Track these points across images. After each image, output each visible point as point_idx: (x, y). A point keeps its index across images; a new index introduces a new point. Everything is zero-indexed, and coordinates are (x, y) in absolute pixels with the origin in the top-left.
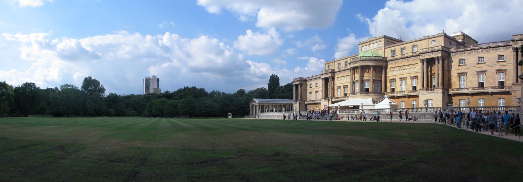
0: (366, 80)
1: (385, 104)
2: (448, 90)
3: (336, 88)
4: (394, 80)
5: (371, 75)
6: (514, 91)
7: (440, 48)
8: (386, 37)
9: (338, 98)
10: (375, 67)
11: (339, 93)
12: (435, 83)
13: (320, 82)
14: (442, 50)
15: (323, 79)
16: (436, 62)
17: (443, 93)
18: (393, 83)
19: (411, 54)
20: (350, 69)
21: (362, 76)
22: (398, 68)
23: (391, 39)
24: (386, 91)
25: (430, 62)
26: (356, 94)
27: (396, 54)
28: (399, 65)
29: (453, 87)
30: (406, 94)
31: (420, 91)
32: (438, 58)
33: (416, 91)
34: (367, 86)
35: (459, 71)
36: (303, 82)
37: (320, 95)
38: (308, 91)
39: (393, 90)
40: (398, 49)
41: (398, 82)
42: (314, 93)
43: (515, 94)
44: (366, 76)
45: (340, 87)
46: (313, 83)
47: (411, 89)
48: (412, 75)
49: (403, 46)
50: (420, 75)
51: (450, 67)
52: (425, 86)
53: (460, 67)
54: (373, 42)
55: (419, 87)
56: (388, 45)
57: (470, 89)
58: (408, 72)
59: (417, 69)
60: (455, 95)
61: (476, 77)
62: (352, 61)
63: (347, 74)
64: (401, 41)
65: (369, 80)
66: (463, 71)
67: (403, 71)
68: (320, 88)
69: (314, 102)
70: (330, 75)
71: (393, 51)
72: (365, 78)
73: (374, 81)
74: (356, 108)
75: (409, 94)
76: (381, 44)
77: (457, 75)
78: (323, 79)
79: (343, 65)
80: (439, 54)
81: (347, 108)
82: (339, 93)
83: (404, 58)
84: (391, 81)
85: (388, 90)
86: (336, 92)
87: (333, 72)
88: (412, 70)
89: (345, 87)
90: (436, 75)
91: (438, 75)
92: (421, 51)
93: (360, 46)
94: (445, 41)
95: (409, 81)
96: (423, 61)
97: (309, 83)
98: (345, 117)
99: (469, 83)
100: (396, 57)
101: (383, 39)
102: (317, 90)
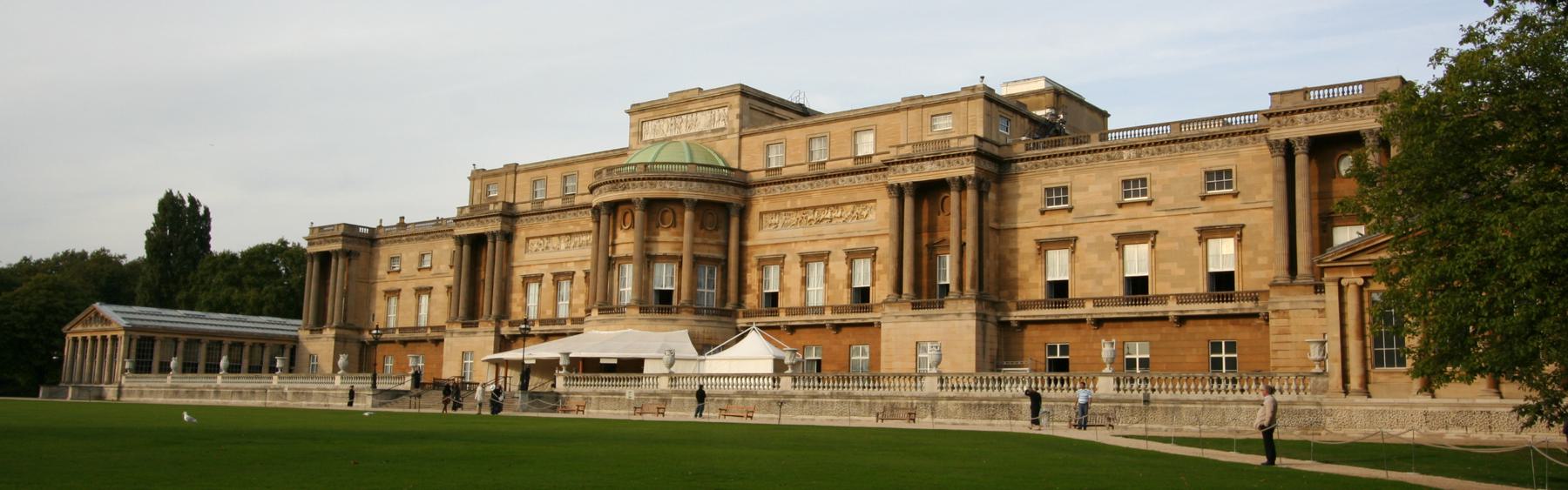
1: (751, 355)
2: (997, 305)
3: (517, 280)
4: (779, 260)
5: (686, 238)
6: (1282, 313)
7: (970, 143)
8: (745, 92)
10: (700, 206)
11: (532, 303)
12: (948, 276)
14: (979, 154)
15: (460, 240)
16: (954, 196)
17: (981, 318)
19: (849, 164)
20: (596, 210)
21: (647, 241)
22: (794, 217)
24: (740, 302)
25: (930, 192)
26: (620, 310)
28: (799, 204)
29: (1022, 296)
30: (828, 316)
31: (887, 309)
32: (962, 183)
33: (869, 309)
34: (664, 277)
35: (1045, 234)
36: (360, 244)
37: (433, 310)
38: (381, 287)
39: (773, 299)
41: (795, 270)
42: (408, 297)
43: (1283, 322)
44: (665, 242)
45: (538, 278)
46: (408, 253)
47: (845, 298)
49: (817, 130)
50: (885, 246)
51: (1004, 211)
53: (1047, 219)
55: (881, 292)
56: (753, 123)
57: (1089, 305)
58: (834, 232)
60: (1023, 324)
61: (1115, 254)
62: (605, 178)
63: (571, 229)
64: (803, 112)
65: (677, 259)
66: (1058, 233)
67: (817, 229)
68: (439, 275)
69: (407, 336)
70: (494, 226)
73: (697, 261)
74: (633, 366)
75: (838, 318)
76: (727, 116)
78: (460, 240)
79: (555, 189)
80: (967, 169)
81: (590, 366)
82: (533, 302)
83: (822, 176)
84: (763, 264)
85: (751, 300)
86: (516, 296)
87: (510, 214)
88: (852, 226)
90: (954, 246)
91: (962, 245)
92: (893, 154)
94: (988, 116)
95: (839, 267)
96: (899, 192)
97: (385, 252)
98: (602, 405)
99: (1083, 278)
101: (736, 99)
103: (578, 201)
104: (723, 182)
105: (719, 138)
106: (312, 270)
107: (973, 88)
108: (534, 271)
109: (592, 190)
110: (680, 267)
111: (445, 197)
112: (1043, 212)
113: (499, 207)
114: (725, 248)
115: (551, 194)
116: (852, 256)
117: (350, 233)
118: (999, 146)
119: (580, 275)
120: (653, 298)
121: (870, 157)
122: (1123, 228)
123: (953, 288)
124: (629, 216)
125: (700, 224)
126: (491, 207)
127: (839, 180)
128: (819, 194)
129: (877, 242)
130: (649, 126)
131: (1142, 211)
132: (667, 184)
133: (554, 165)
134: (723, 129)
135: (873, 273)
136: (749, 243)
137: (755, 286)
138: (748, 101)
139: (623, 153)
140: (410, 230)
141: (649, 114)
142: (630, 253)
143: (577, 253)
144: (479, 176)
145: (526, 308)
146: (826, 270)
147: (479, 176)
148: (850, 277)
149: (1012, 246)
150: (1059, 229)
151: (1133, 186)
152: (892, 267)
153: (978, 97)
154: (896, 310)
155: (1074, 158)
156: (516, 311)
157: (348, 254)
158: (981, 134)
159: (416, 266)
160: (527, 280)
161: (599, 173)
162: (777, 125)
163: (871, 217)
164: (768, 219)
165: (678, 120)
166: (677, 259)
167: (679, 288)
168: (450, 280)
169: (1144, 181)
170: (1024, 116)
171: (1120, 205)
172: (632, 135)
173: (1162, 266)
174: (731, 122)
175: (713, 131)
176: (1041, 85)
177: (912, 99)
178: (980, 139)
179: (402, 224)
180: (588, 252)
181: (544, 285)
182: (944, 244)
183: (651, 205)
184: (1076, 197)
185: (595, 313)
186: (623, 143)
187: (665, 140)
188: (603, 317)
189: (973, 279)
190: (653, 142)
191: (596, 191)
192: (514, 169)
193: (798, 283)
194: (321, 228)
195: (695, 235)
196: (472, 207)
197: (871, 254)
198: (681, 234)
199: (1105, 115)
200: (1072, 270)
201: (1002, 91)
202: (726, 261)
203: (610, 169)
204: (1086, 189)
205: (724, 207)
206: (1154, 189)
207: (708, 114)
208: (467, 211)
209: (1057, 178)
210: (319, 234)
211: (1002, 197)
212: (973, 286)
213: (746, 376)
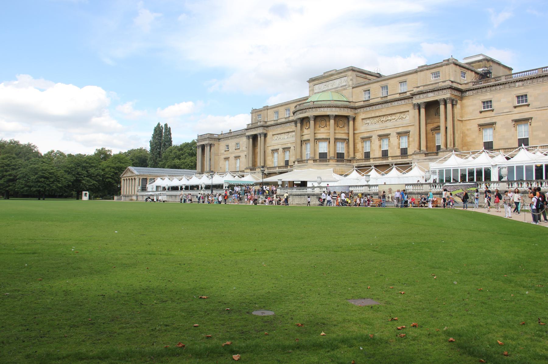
3: (269, 151)
4: (369, 138)
5: (332, 130)
8: (353, 70)
10: (336, 117)
15: (248, 137)
16: (442, 107)
19: (397, 96)
20: (295, 122)
25: (432, 107)
27: (371, 97)
28: (377, 114)
31: (414, 157)
32: (445, 102)
34: (323, 148)
35: (482, 122)
42: (232, 159)
44: (322, 133)
45: (277, 150)
46: (232, 143)
47: (398, 153)
48: (400, 130)
49: (383, 83)
50: (414, 131)
52: (423, 148)
53: (483, 115)
54: (332, 78)
59: (410, 118)
61: (513, 129)
62: (298, 108)
63: (289, 130)
64: (379, 76)
66: (488, 121)
68: (243, 151)
73: (336, 140)
77: (477, 128)
78: (248, 137)
80: (447, 95)
82: (276, 160)
83: (386, 102)
86: (269, 158)
88: (399, 123)
89: (286, 149)
92: (416, 90)
100: (371, 102)
102: (237, 155)
103: (291, 119)
105: (344, 89)
106: (199, 151)
107: (448, 60)
108: (276, 148)
109: (294, 113)
111: (241, 121)
112: (481, 112)
115: (280, 117)
116: (400, 134)
117: (211, 137)
118: (461, 84)
120: (317, 157)
121: (406, 92)
122: (517, 117)
123: (442, 147)
126: (259, 123)
127: (393, 103)
130: (317, 86)
131: (525, 109)
132: (322, 109)
133: (281, 105)
134: (346, 85)
135: (409, 142)
136: (355, 132)
137: (360, 150)
139: (306, 98)
140: (232, 134)
141: (316, 82)
142: (309, 138)
144: (255, 112)
145: (273, 162)
147: (255, 112)
148: (399, 144)
149: (468, 127)
150: (488, 119)
151: (522, 98)
152: (417, 138)
153: (451, 64)
154: (418, 157)
155: (494, 88)
156: (269, 163)
158: (452, 80)
159: (234, 148)
160: (275, 151)
161: (296, 107)
163: (407, 118)
165: (327, 83)
166: (327, 140)
167: (329, 152)
169: (526, 96)
170: (472, 71)
171: (515, 107)
172: (310, 91)
173: (535, 133)
175: (342, 87)
176: (481, 58)
177: (422, 66)
178: (452, 82)
179: (230, 133)
180: (294, 139)
181: (279, 153)
182: (437, 129)
183: (316, 118)
184: (494, 104)
185: (296, 163)
186: (307, 95)
188: (299, 164)
189: (451, 142)
190: (318, 93)
191: (295, 114)
192: (267, 108)
193: (378, 147)
194: (201, 136)
195: (335, 130)
196: (252, 124)
197: (407, 133)
199: (511, 69)
200: (494, 137)
201: (462, 62)
202: (348, 139)
203: (299, 105)
204: (499, 101)
205: (347, 117)
206: (529, 98)
208: (250, 126)
209: (487, 96)
210: (201, 138)
211: (462, 107)
212: (450, 145)
213: (356, 186)
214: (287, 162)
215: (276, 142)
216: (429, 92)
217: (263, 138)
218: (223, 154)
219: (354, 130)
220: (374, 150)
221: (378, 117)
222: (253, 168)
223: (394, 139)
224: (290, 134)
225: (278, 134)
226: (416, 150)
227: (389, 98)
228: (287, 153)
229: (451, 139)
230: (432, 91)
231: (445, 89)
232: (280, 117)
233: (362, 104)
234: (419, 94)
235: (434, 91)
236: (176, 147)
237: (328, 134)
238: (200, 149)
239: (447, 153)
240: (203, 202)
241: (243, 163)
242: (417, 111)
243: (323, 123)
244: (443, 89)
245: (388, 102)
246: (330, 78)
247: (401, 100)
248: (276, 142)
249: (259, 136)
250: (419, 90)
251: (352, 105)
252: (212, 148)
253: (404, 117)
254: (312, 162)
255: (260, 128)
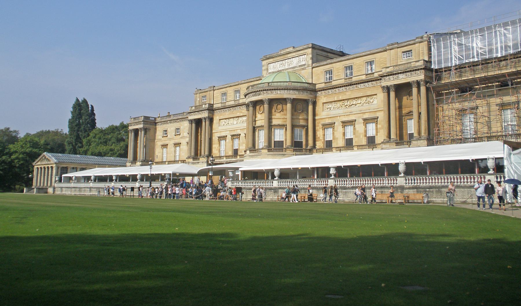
0: (279, 125)
3: (215, 138)
4: (331, 125)
5: (289, 116)
8: (314, 47)
9: (220, 157)
10: (294, 101)
11: (222, 149)
13: (185, 126)
15: (191, 121)
16: (415, 90)
18: (329, 131)
19: (364, 77)
20: (247, 105)
22: (339, 104)
23: (323, 49)
25: (402, 90)
27: (334, 78)
28: (341, 98)
32: (418, 83)
34: (279, 135)
40: (338, 67)
41: (339, 128)
42: (171, 147)
45: (224, 138)
46: (171, 128)
48: (366, 116)
50: (382, 116)
56: (317, 61)
58: (358, 110)
62: (251, 90)
70: (205, 114)
71: (330, 72)
72: (275, 122)
76: (306, 58)
78: (191, 121)
80: (420, 76)
82: (223, 148)
83: (351, 85)
84: (326, 126)
85: (320, 144)
86: (215, 146)
87: (211, 109)
89: (235, 137)
92: (384, 71)
93: (264, 63)
96: (388, 89)
97: (160, 129)
100: (334, 83)
101: (310, 50)
102: (177, 141)
103: (241, 101)
104: (304, 90)
105: (303, 69)
106: (131, 136)
108: (223, 134)
110: (286, 130)
113: (207, 106)
114: (307, 120)
116: (366, 121)
119: (243, 135)
123: (416, 135)
124: (262, 107)
125: (294, 109)
126: (204, 106)
127: (359, 86)
128: (350, 92)
129: (378, 114)
132: (279, 92)
134: (304, 65)
135: (377, 129)
136: (316, 118)
138: (315, 51)
140: (172, 118)
142: (263, 124)
143: (240, 125)
145: (220, 151)
146: (354, 129)
148: (366, 131)
152: (386, 126)
156: (215, 152)
157: (146, 130)
159: (174, 134)
161: (248, 88)
162: (329, 61)
163: (375, 102)
164: (326, 106)
167: (286, 140)
168: (187, 140)
174: (308, 62)
175: (300, 66)
179: (169, 116)
180: (245, 125)
183: (271, 102)
185: (248, 152)
187: (278, 71)
190: (273, 72)
191: (247, 97)
193: (342, 135)
195: (292, 115)
197: (375, 120)
198: (286, 115)
202: (307, 126)
205: (306, 102)
207: (297, 58)
212: (425, 133)
214: (236, 152)
215: (224, 127)
216: (401, 73)
217: (207, 123)
218: (160, 140)
219: (314, 115)
220: (337, 138)
221: (341, 100)
222: (196, 156)
223: (360, 127)
224: (240, 119)
225: (226, 119)
226: (385, 138)
227: (354, 79)
228: (236, 141)
229: (425, 127)
230: (403, 73)
231: (418, 70)
232: (229, 99)
233: (323, 85)
234: (389, 75)
235: (406, 72)
236: (102, 131)
237: (284, 120)
238: (133, 134)
239: (422, 141)
240: (160, 197)
241: (184, 151)
242: (386, 94)
243: (280, 106)
244: (416, 70)
245: (353, 85)
246: (286, 56)
247: (367, 82)
248: (224, 127)
249: (203, 121)
250: (388, 70)
251: (312, 87)
252: (148, 133)
253: (371, 101)
254: (266, 151)
255: (205, 111)
